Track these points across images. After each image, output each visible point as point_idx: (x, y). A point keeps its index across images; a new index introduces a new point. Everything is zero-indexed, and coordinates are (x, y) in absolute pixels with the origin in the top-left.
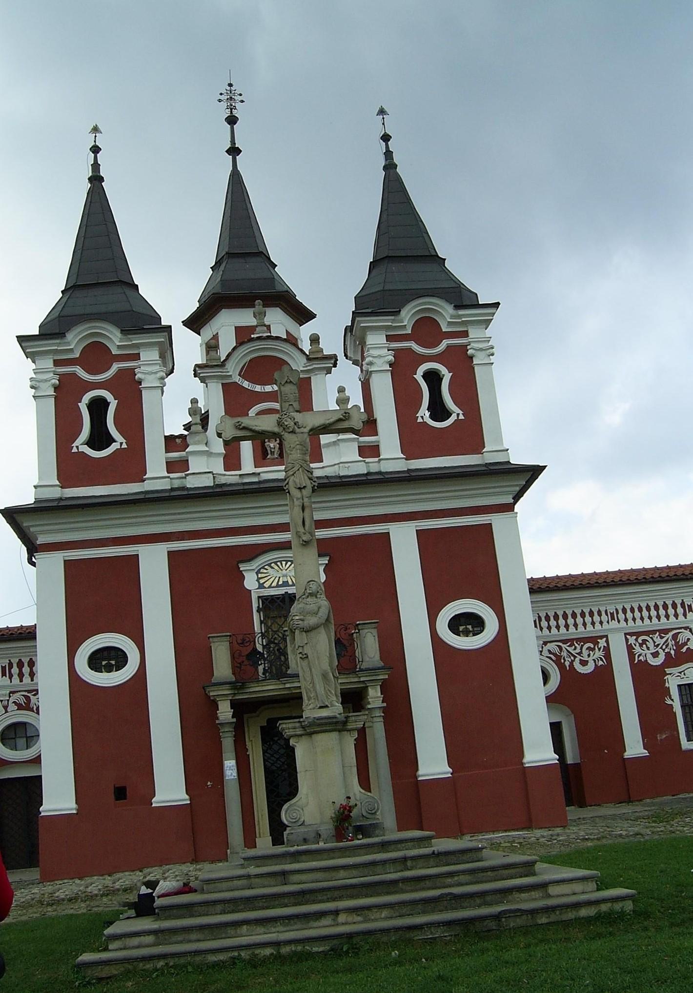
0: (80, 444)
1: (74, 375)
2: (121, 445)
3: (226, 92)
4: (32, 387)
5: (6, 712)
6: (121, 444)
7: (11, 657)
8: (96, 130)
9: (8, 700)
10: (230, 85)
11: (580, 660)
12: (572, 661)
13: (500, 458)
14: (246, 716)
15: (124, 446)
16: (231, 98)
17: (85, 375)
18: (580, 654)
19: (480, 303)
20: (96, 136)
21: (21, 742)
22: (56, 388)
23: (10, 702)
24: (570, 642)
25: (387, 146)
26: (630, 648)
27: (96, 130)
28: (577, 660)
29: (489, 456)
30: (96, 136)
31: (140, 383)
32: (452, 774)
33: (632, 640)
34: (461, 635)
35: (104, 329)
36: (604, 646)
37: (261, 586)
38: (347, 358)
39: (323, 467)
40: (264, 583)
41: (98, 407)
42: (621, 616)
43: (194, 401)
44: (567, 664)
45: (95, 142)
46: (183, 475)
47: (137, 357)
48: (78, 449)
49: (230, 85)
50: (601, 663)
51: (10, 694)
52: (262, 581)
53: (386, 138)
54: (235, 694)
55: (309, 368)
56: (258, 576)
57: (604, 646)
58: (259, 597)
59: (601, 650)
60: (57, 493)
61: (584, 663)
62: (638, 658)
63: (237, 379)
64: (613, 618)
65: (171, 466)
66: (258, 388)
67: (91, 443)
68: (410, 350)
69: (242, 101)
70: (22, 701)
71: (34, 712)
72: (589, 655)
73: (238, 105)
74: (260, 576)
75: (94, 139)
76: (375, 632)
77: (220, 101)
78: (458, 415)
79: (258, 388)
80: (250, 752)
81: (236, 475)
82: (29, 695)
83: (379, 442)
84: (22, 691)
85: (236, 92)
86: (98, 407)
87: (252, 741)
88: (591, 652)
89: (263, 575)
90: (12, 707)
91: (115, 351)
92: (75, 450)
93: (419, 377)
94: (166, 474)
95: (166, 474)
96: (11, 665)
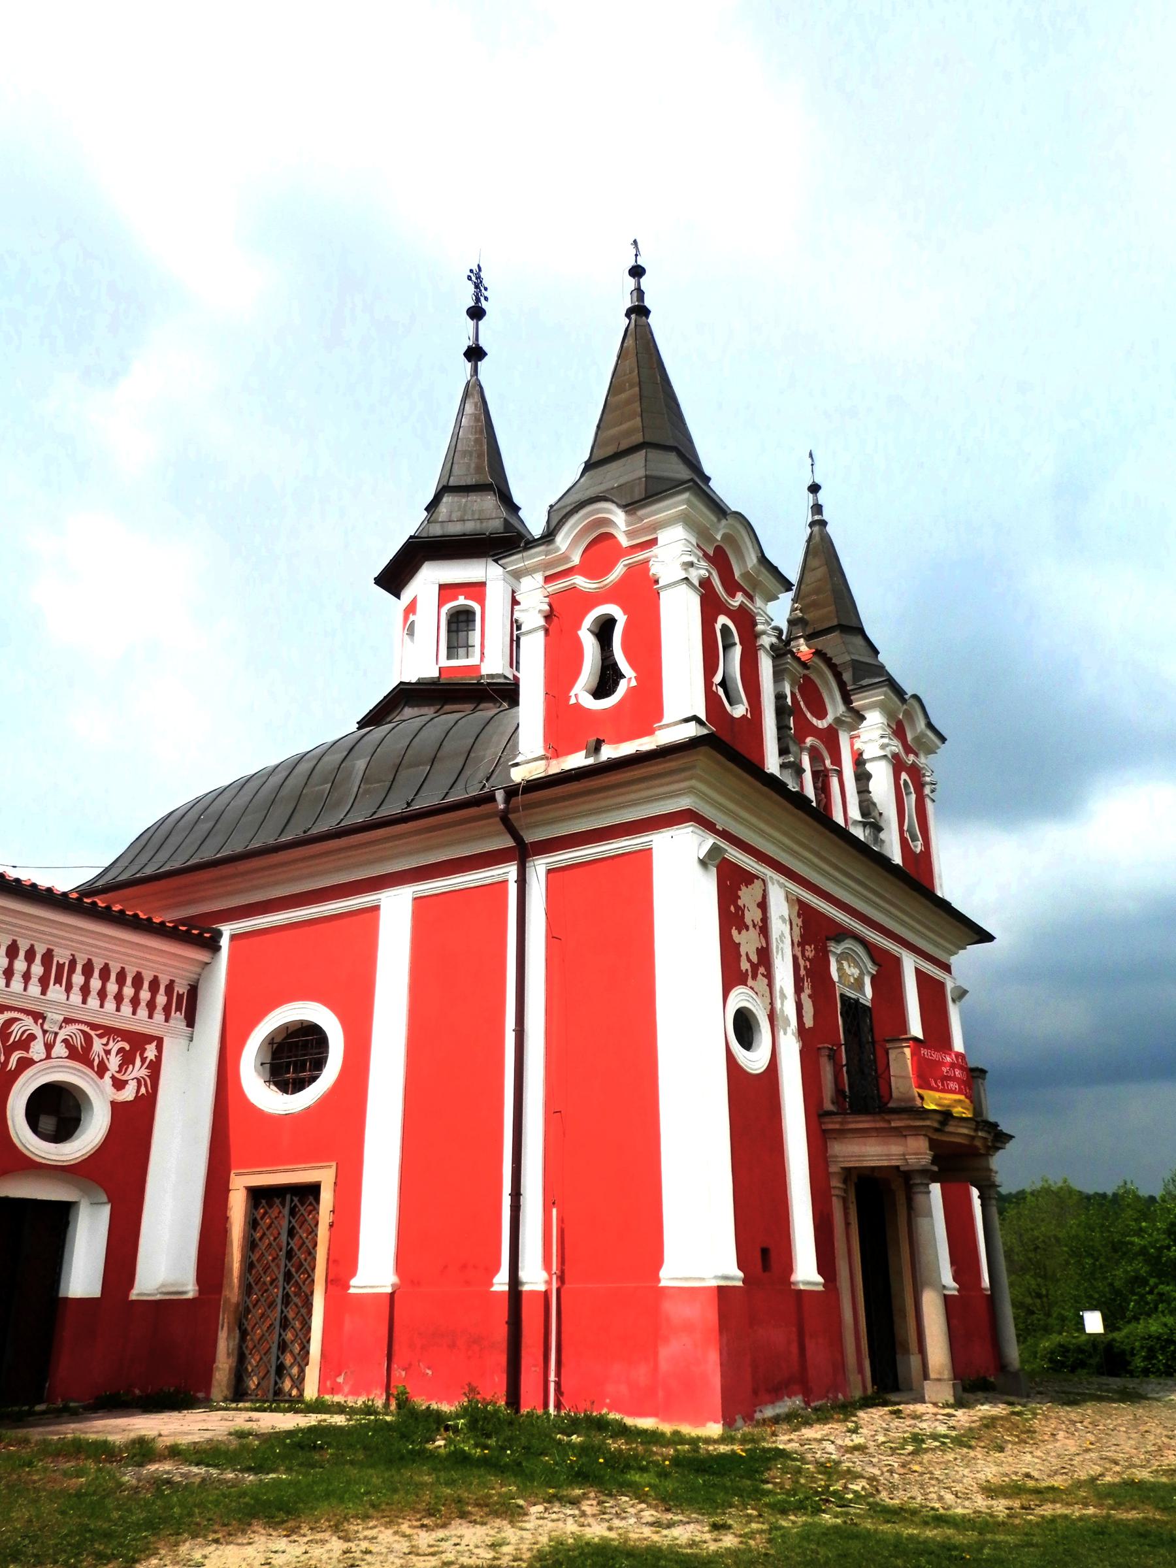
5: (48, 1057)
9: (56, 1034)
21: (48, 1123)
23: (60, 1038)
45: (636, 261)
53: (814, 488)
66: (809, 715)
70: (79, 1041)
71: (93, 1069)
73: (482, 299)
79: (809, 715)
82: (92, 1033)
90: (60, 1050)
96: (73, 963)
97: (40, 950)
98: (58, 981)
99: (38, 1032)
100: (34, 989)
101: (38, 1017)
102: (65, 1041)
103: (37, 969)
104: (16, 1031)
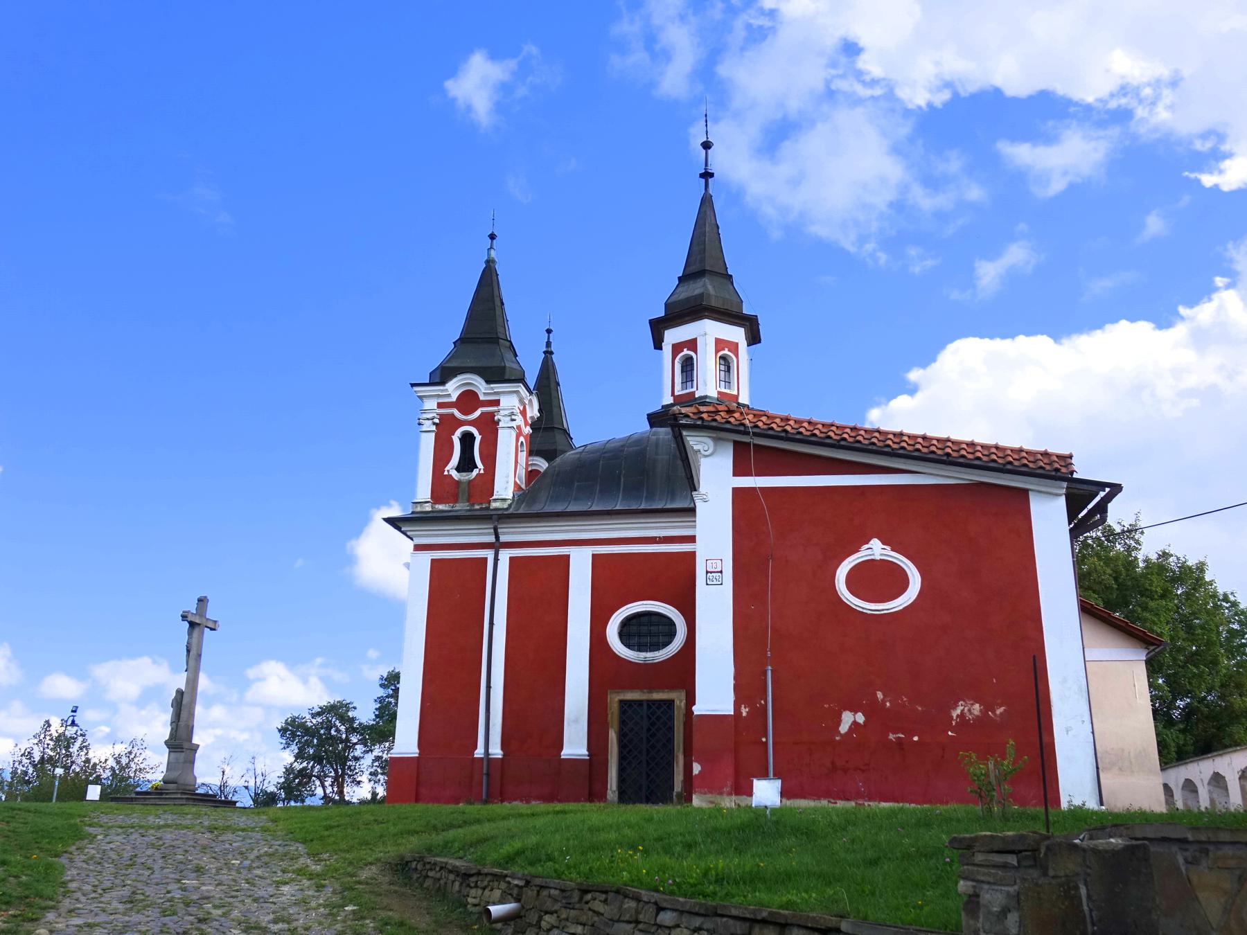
0: (451, 469)
6: (480, 470)
35: (474, 380)
47: (497, 403)
67: (458, 469)
86: (467, 439)
91: (482, 398)
92: (446, 473)
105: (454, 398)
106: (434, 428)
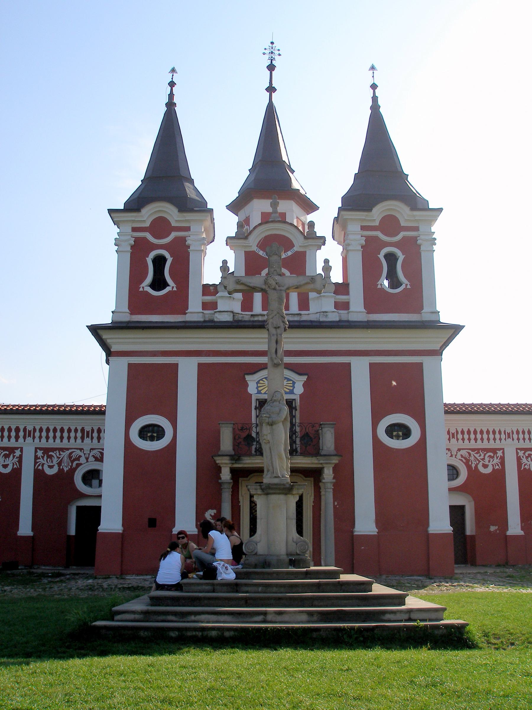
1: (145, 239)
2: (172, 289)
3: (269, 47)
4: (116, 245)
5: (87, 462)
6: (173, 287)
7: (56, 425)
8: (173, 70)
9: (89, 454)
10: (272, 43)
11: (483, 464)
12: (477, 464)
13: (433, 318)
14: (240, 479)
15: (175, 289)
16: (272, 52)
17: (151, 239)
18: (483, 459)
19: (430, 207)
20: (173, 75)
22: (132, 247)
23: (90, 455)
24: (477, 450)
25: (374, 93)
26: (519, 459)
27: (173, 70)
28: (481, 464)
29: (425, 316)
30: (173, 75)
31: (189, 247)
32: (377, 533)
33: (521, 453)
34: (394, 438)
36: (501, 456)
37: (259, 392)
38: (334, 240)
39: (308, 314)
40: (261, 390)
41: (159, 262)
42: (515, 436)
43: (225, 262)
44: (473, 466)
45: (172, 79)
46: (212, 312)
47: (188, 229)
48: (143, 289)
49: (272, 43)
50: (497, 467)
51: (90, 450)
52: (260, 389)
53: (374, 87)
54: (233, 463)
55: (305, 245)
56: (257, 385)
57: (501, 456)
58: (257, 399)
59: (499, 458)
60: (126, 317)
61: (485, 466)
62: (524, 466)
63: (254, 248)
64: (509, 437)
65: (205, 306)
68: (377, 238)
69: (280, 55)
72: (489, 461)
73: (277, 57)
74: (259, 385)
75: (171, 77)
76: (333, 431)
77: (264, 54)
78: (406, 285)
80: (241, 504)
81: (249, 315)
83: (349, 299)
84: (99, 449)
85: (276, 48)
86: (159, 262)
87: (243, 496)
88: (491, 459)
89: (261, 385)
90: (91, 459)
91: (174, 224)
92: (141, 289)
93: (381, 256)
94: (202, 311)
95: (202, 311)
96: (93, 431)
97: (79, 428)
98: (88, 436)
99: (82, 454)
100: (79, 440)
101: (81, 449)
102: (93, 456)
103: (79, 434)
104: (74, 455)
105: (147, 224)
106: (129, 249)
